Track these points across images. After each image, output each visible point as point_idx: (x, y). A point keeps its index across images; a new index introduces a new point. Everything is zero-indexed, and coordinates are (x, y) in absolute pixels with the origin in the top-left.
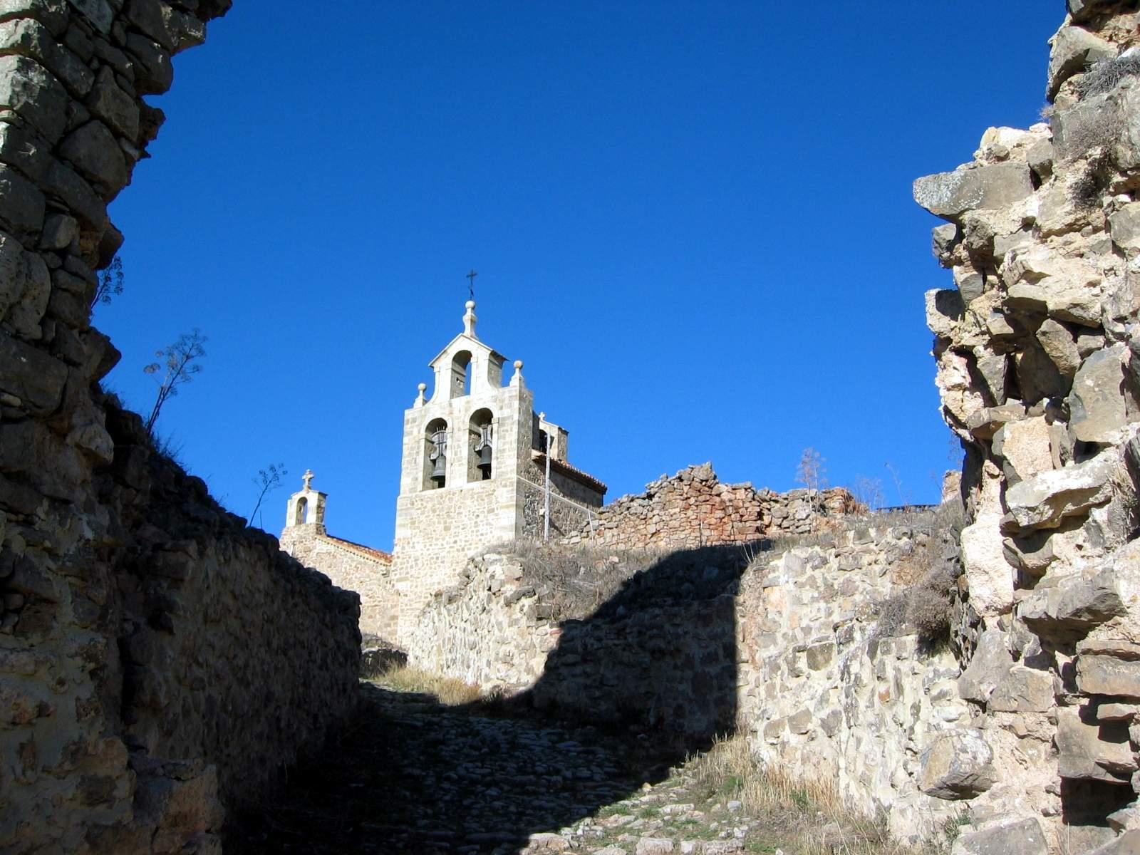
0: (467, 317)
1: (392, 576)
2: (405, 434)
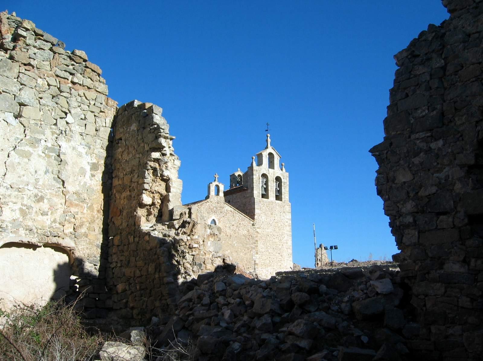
0: (269, 140)
1: (256, 226)
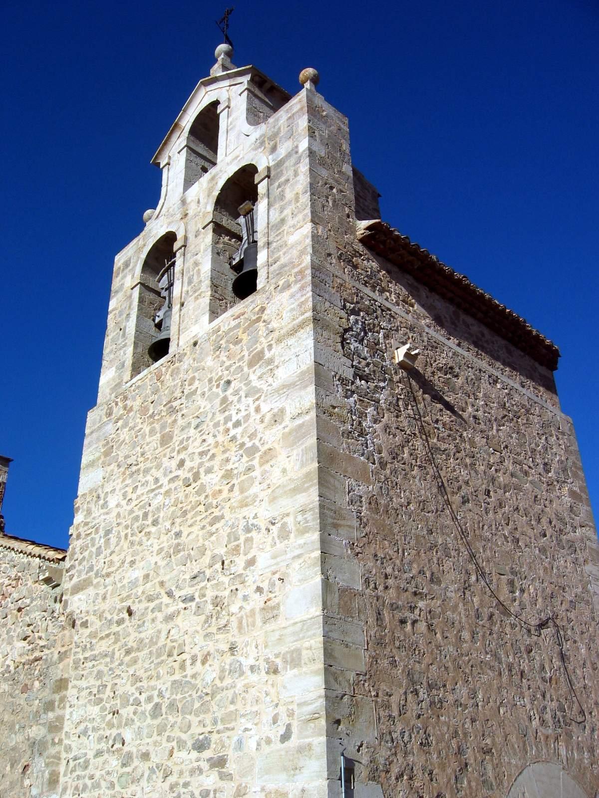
2: (112, 294)
